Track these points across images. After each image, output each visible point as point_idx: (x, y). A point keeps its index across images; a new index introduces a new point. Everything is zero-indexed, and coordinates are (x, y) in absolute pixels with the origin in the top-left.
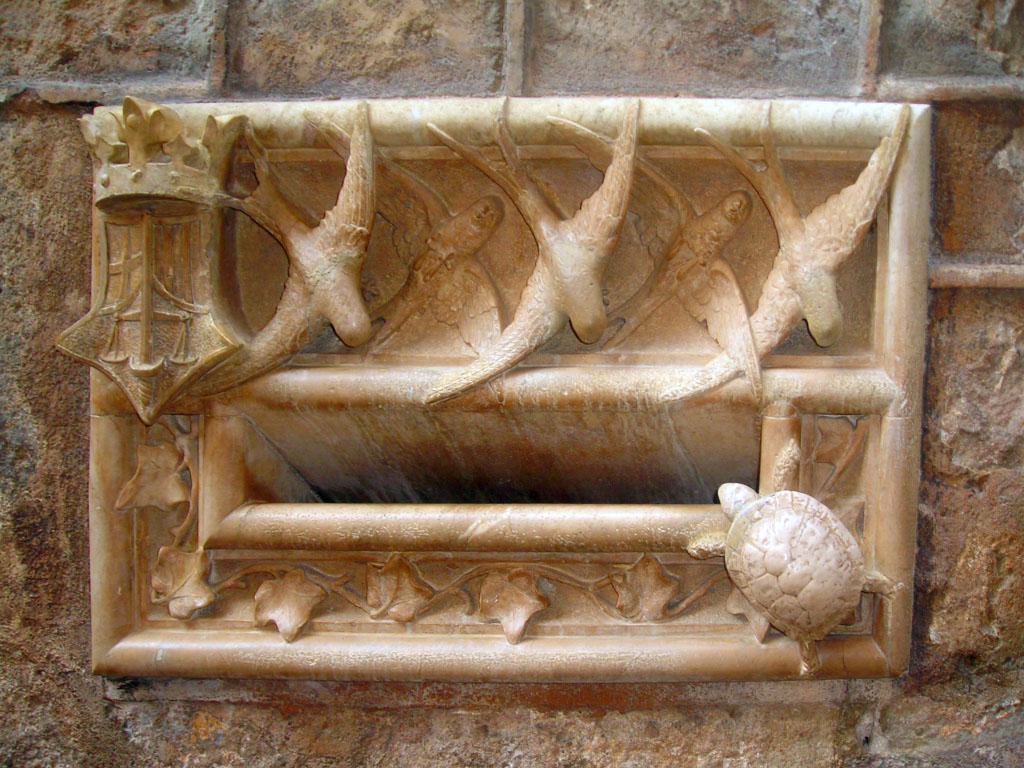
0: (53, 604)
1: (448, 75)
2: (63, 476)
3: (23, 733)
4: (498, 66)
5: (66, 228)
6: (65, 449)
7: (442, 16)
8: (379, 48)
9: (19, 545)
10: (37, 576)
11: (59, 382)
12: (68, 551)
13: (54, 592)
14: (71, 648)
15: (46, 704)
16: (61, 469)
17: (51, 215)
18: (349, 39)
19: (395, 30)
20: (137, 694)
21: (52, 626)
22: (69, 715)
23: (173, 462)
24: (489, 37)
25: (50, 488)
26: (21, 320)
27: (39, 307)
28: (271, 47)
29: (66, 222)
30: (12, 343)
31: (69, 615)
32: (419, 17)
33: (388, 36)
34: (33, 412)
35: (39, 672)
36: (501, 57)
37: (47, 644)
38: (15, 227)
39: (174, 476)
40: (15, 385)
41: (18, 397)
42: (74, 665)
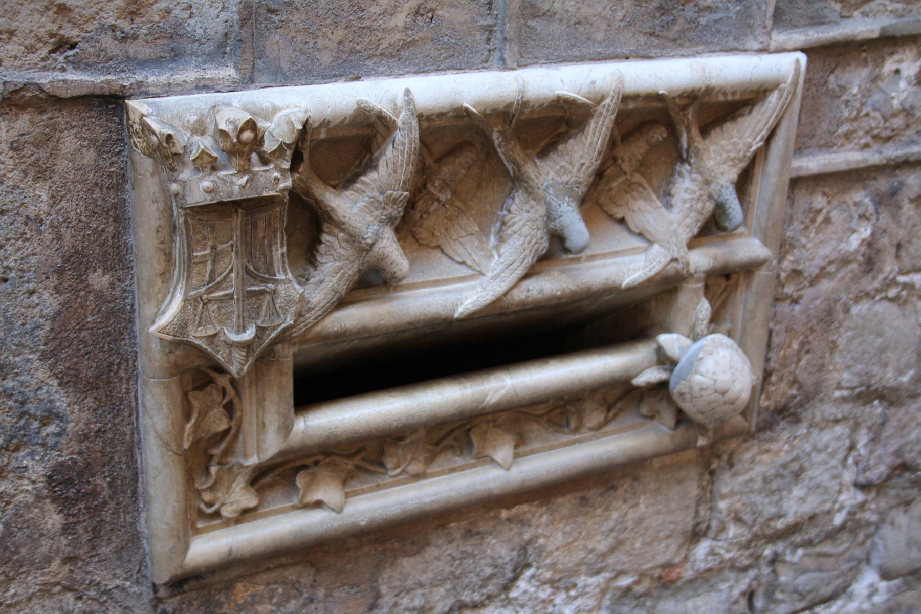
8: (392, 30)
9: (54, 500)
10: (75, 520)
12: (106, 493)
13: (94, 529)
14: (114, 569)
16: (95, 427)
17: (63, 203)
18: (367, 23)
19: (406, 14)
24: (482, 16)
26: (37, 305)
27: (57, 290)
29: (83, 209)
30: (28, 327)
33: (401, 19)
34: (60, 385)
38: (21, 219)
40: (37, 364)
41: (42, 374)
42: (118, 582)
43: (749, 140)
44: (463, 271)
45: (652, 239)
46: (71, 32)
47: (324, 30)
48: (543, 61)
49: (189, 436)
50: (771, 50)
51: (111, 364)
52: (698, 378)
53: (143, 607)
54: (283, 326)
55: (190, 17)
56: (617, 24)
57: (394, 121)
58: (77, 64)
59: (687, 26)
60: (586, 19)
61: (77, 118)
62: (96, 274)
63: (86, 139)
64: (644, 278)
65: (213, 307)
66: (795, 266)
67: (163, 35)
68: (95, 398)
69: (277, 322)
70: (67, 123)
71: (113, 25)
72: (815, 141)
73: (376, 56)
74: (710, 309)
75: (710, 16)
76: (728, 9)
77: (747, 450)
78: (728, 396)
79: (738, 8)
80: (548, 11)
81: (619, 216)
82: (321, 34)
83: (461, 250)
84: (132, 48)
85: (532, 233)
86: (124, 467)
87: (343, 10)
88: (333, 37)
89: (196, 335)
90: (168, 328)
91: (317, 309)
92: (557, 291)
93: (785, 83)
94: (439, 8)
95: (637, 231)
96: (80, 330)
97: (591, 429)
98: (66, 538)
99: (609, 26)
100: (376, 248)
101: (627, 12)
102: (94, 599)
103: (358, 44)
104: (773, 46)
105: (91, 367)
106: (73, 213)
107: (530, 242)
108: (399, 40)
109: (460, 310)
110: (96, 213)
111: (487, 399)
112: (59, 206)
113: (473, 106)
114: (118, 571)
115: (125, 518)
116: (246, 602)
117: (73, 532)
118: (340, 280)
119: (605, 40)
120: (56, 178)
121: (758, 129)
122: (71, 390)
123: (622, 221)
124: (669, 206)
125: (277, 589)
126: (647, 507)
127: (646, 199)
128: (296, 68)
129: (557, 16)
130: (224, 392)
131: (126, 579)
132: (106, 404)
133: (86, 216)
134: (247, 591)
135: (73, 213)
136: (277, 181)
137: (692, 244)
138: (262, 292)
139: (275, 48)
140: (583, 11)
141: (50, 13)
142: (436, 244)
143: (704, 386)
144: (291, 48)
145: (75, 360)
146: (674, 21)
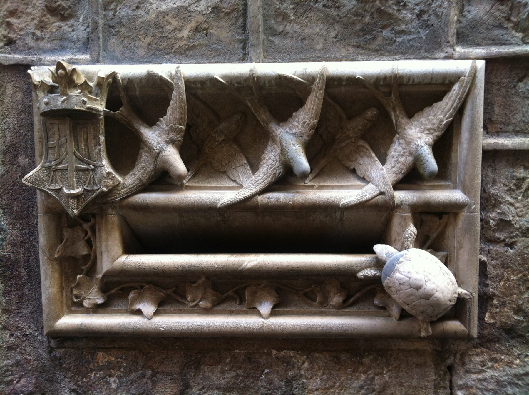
0: (18, 302)
1: (218, 53)
2: (21, 242)
3: (3, 364)
4: (244, 48)
5: (16, 125)
6: (21, 230)
7: (213, 23)
8: (181, 39)
10: (10, 289)
11: (17, 198)
12: (26, 278)
13: (19, 297)
14: (29, 323)
15: (16, 350)
17: (7, 119)
18: (165, 34)
19: (189, 30)
20: (66, 344)
21: (18, 313)
22: (29, 355)
23: (82, 235)
24: (239, 34)
25: (15, 248)
28: (123, 39)
29: (16, 122)
31: (27, 308)
32: (201, 23)
33: (185, 33)
34: (3, 213)
35: (12, 335)
36: (245, 44)
37: (16, 321)
39: (82, 243)
43: (441, 116)
44: (234, 185)
45: (368, 180)
46: (12, 35)
47: (139, 37)
48: (280, 61)
49: (59, 251)
50: (455, 58)
51: (29, 207)
52: (398, 275)
53: (43, 350)
54: (99, 191)
55: (73, 31)
56: (331, 40)
57: (171, 83)
58: (15, 52)
59: (385, 42)
60: (309, 36)
61: (14, 76)
62: (22, 157)
63: (18, 87)
64: (357, 201)
65: (59, 174)
66: (503, 217)
67: (56, 38)
68: (20, 224)
69: (96, 188)
70: (9, 79)
71: (33, 33)
72: (511, 128)
73: (172, 53)
74: (415, 230)
75: (405, 37)
76: (419, 32)
77: (478, 355)
78: (421, 291)
79: (428, 31)
80: (283, 31)
81: (352, 167)
82: (137, 39)
83: (236, 174)
84: (41, 44)
85: (273, 163)
86: (35, 265)
87: (150, 27)
88: (145, 41)
89: (50, 188)
90: (28, 179)
91: (128, 188)
92: (290, 201)
93: (465, 76)
94: (210, 28)
95: (362, 176)
96: (14, 185)
97: (334, 307)
98: (5, 298)
99: (326, 41)
100: (160, 156)
101: (338, 32)
102: (19, 338)
103: (160, 46)
104: (456, 55)
105: (19, 206)
106: (11, 124)
107: (271, 168)
108: (186, 45)
109: (221, 203)
110: (22, 126)
111: (244, 265)
112: (6, 120)
113: (222, 78)
114: (31, 325)
115: (35, 295)
116: (104, 365)
117: (9, 296)
118: (143, 173)
119: (323, 49)
120: (4, 106)
121: (446, 109)
122: (8, 217)
123: (354, 171)
124: (383, 162)
125: (122, 362)
126: (390, 378)
127: (368, 157)
128: (124, 57)
129: (289, 35)
130: (86, 233)
131: (36, 331)
132: (27, 228)
133: (17, 127)
134: (105, 359)
135: (11, 124)
136: (84, 103)
137: (398, 186)
138: (87, 170)
139: (113, 45)
140: (306, 31)
141: (4, 26)
142: (223, 170)
143: (401, 282)
144: (122, 46)
145: (10, 201)
146: (374, 38)
